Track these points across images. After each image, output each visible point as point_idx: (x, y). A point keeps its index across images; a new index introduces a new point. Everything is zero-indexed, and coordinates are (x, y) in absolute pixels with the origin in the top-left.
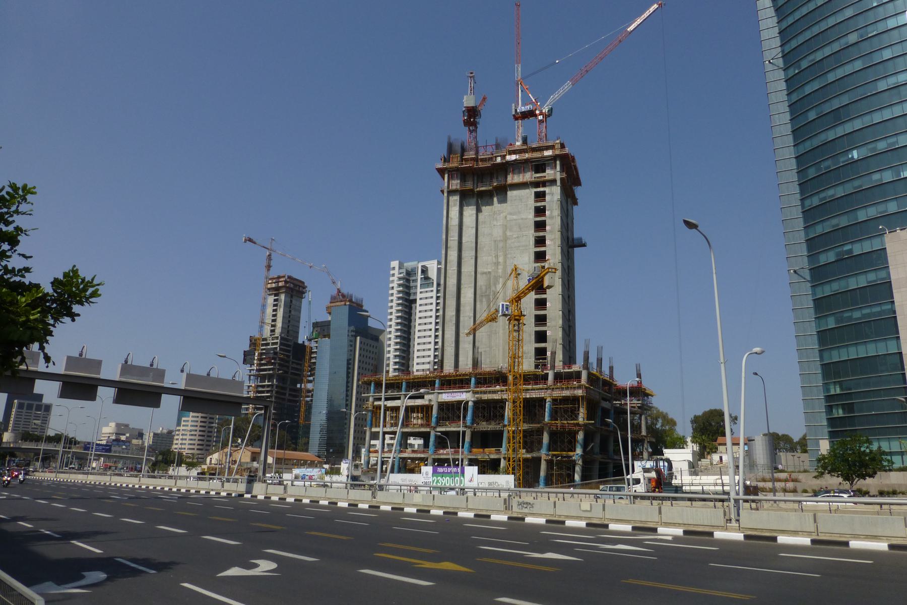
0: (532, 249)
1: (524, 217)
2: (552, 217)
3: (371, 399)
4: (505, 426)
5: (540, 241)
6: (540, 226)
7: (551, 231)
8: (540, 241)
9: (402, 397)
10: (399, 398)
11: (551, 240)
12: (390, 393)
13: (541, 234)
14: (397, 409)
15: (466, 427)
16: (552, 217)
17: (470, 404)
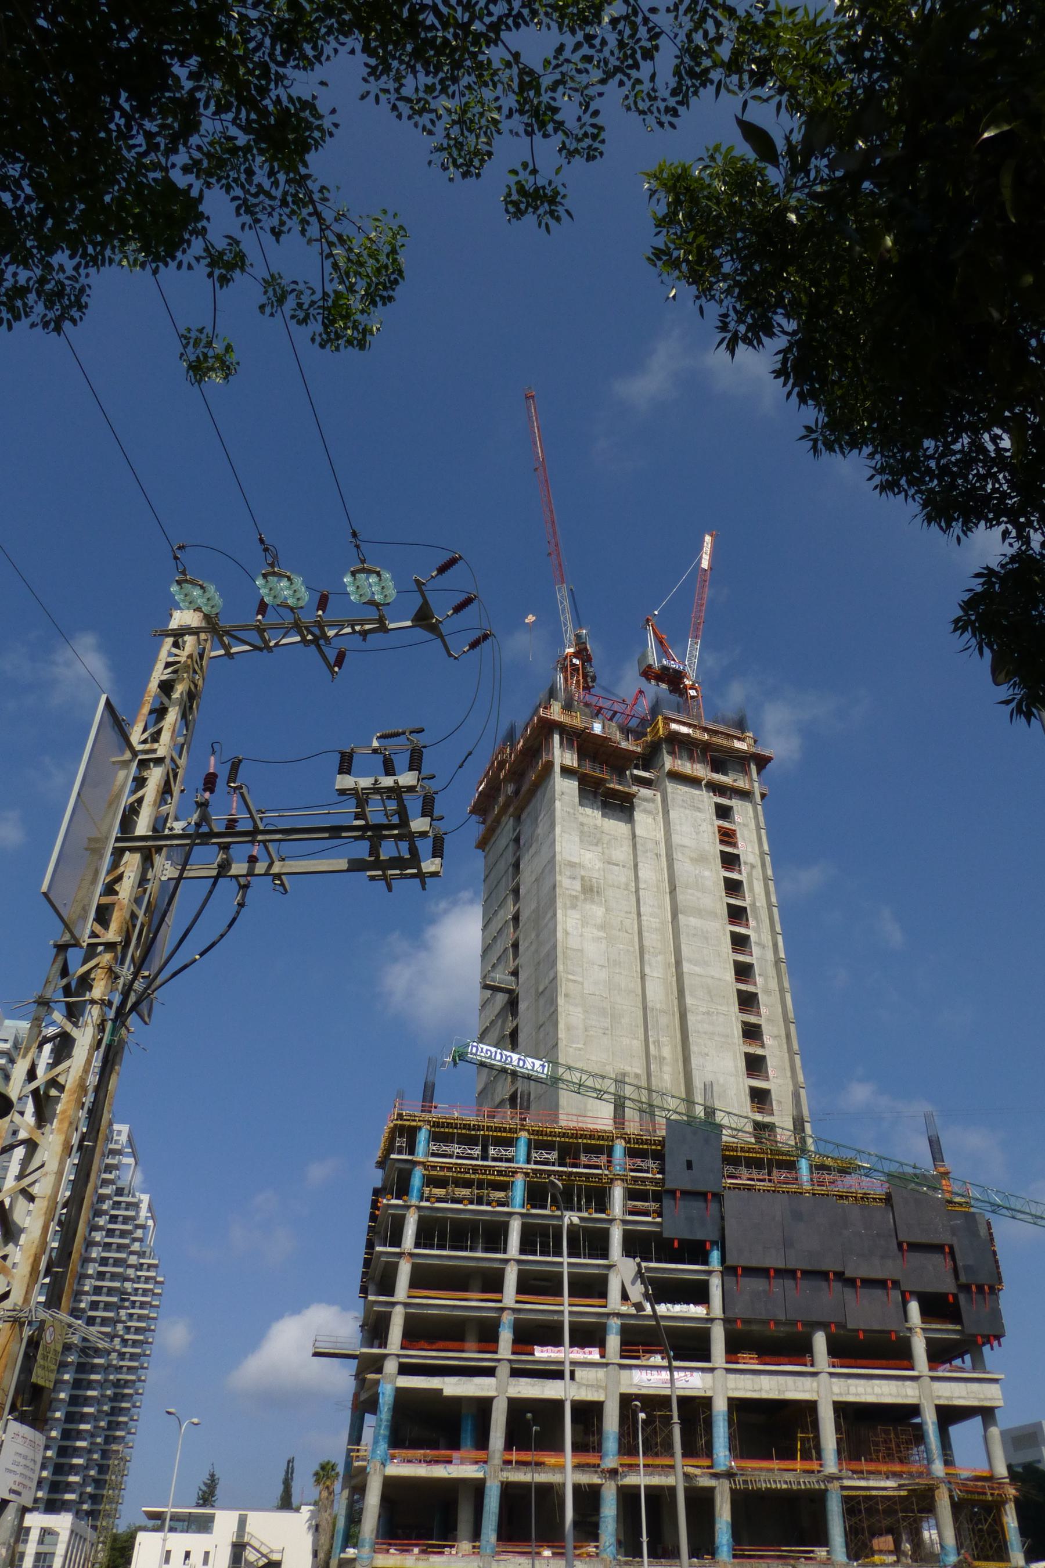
0: (742, 1047)
1: (717, 976)
2: (767, 992)
3: (391, 1366)
4: (832, 1478)
5: (752, 1033)
6: (747, 1001)
7: (769, 1020)
8: (752, 1033)
9: (503, 1370)
10: (490, 1372)
11: (775, 1037)
12: (418, 1356)
13: (752, 1019)
14: (483, 1406)
15: (716, 1476)
16: (767, 992)
17: (720, 1407)
